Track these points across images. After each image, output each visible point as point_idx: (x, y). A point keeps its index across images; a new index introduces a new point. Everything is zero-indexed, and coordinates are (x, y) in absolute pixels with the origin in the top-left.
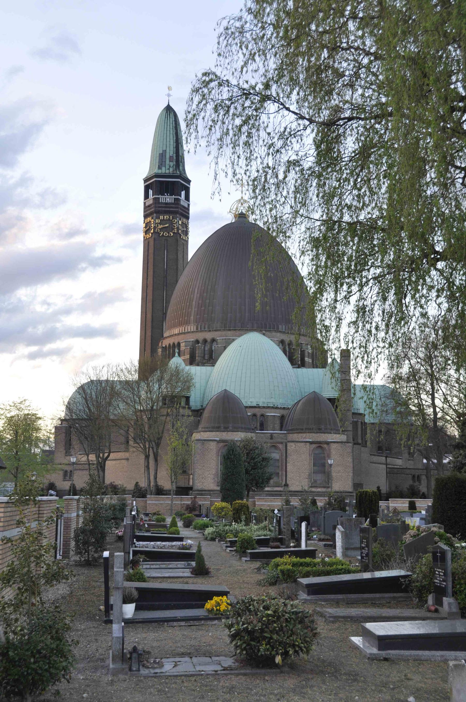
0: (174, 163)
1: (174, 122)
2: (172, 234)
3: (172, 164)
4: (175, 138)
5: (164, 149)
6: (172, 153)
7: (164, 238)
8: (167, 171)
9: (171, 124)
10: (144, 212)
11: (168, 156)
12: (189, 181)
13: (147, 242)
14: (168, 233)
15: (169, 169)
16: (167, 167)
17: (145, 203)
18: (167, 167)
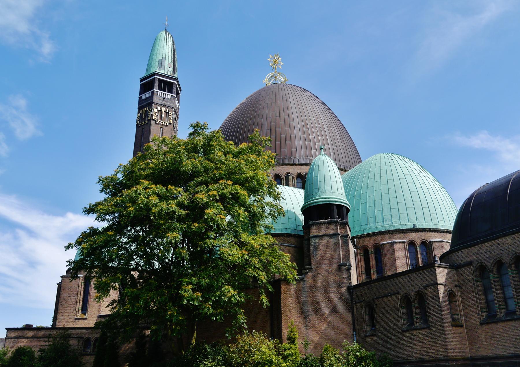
0: (172, 69)
1: (172, 41)
2: (168, 124)
3: (170, 69)
4: (173, 52)
5: (164, 56)
6: (170, 61)
7: (160, 126)
8: (166, 73)
9: (170, 42)
10: (138, 106)
11: (167, 63)
12: (181, 90)
13: (141, 128)
14: (165, 122)
15: (167, 72)
16: (166, 70)
17: (140, 98)
18: (166, 70)
